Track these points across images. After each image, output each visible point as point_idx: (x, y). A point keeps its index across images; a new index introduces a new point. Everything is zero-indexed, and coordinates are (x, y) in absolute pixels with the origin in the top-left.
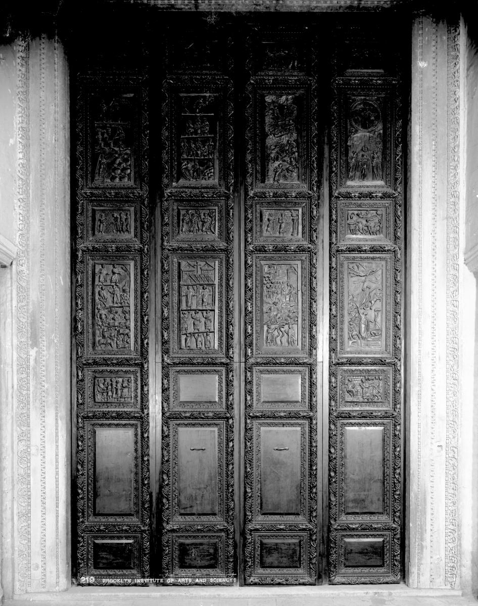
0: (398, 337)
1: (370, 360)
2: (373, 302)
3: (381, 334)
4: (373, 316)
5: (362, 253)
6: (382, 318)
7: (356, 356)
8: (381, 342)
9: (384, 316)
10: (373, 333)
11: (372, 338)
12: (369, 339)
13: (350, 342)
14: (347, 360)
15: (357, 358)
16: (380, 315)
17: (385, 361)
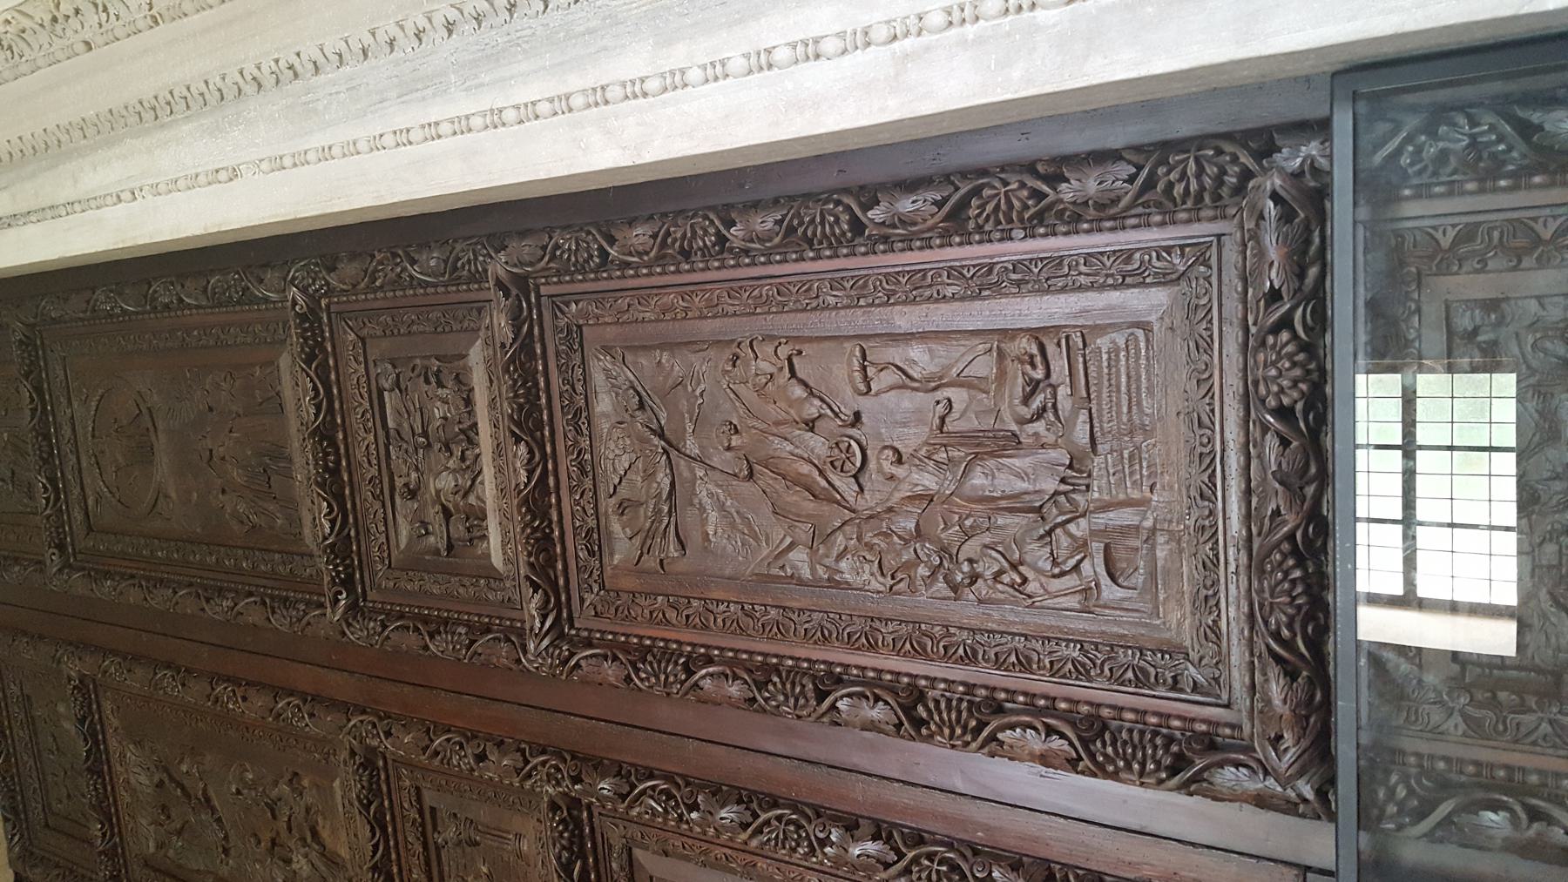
0: (1038, 195)
1: (1271, 442)
2: (813, 409)
3: (1036, 334)
4: (908, 402)
5: (551, 481)
6: (908, 337)
7: (1234, 558)
8: (1101, 330)
9: (904, 318)
10: (1026, 400)
11: (1065, 404)
12: (1081, 434)
13: (1110, 592)
14: (1274, 670)
15: (1256, 566)
16: (894, 354)
17: (1274, 296)
